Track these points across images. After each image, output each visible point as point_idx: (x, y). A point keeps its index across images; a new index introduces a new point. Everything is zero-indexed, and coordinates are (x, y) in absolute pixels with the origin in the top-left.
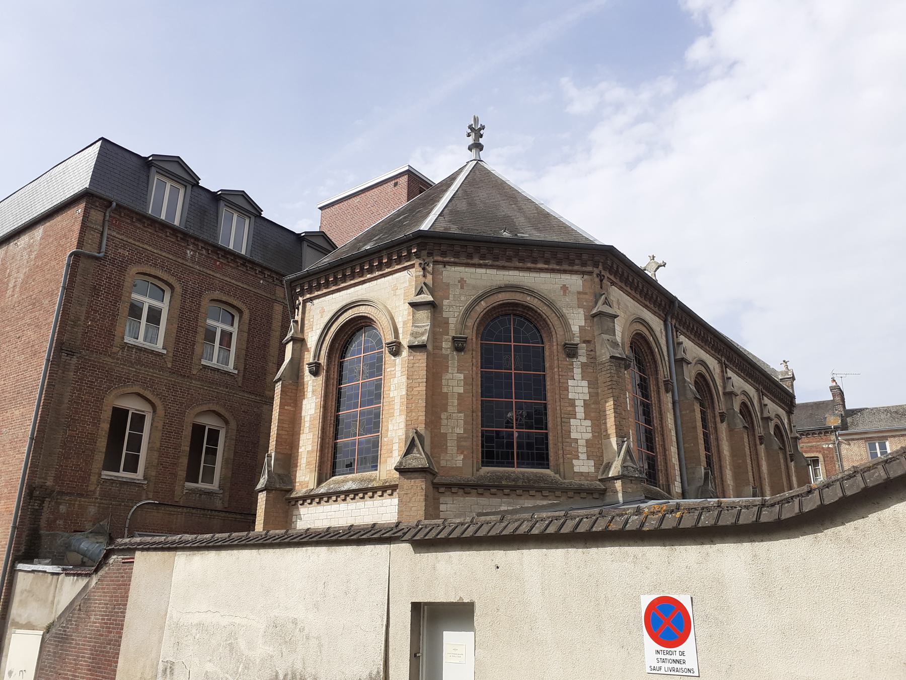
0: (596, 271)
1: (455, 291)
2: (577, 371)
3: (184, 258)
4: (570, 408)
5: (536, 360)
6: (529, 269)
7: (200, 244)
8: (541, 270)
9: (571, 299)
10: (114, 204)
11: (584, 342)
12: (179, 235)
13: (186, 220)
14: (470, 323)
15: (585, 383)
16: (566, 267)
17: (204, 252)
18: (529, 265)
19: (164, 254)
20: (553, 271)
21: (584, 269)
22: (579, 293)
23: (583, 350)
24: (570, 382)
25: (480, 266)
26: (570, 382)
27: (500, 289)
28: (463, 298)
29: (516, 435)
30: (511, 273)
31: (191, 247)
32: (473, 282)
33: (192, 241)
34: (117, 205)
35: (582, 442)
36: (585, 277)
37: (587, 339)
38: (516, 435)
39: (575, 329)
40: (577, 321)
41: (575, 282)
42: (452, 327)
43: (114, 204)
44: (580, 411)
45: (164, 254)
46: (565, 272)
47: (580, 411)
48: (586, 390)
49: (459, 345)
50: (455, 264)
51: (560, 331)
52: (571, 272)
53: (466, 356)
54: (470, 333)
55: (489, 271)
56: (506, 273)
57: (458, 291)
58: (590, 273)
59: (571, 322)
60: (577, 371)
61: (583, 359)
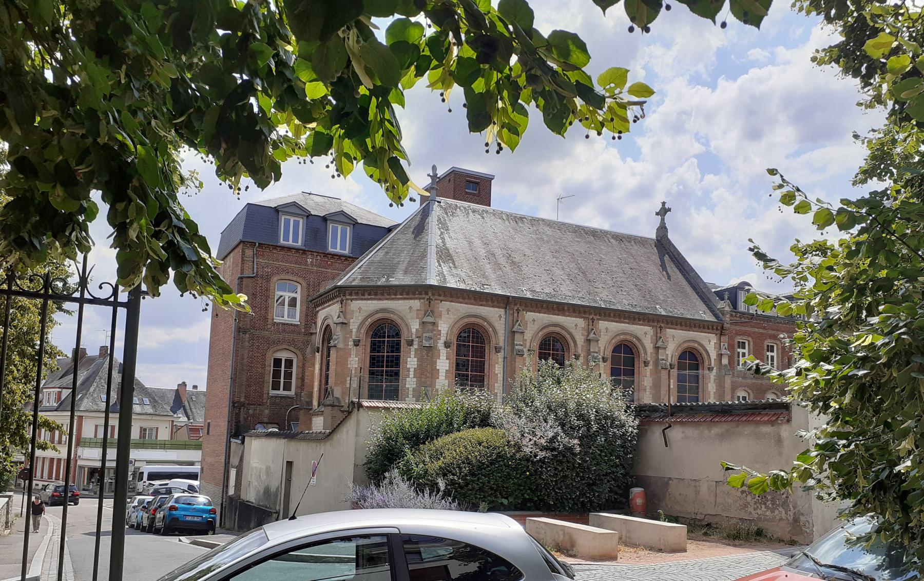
0: (427, 297)
1: (357, 314)
2: (413, 353)
3: (306, 265)
4: (407, 373)
5: (396, 347)
6: (393, 299)
7: (315, 254)
8: (399, 299)
9: (414, 314)
10: (257, 244)
11: (417, 337)
12: (301, 251)
13: (306, 242)
14: (363, 331)
15: (416, 359)
16: (411, 296)
17: (319, 257)
18: (393, 297)
19: (293, 265)
20: (405, 299)
21: (421, 296)
22: (417, 310)
23: (416, 343)
24: (409, 359)
25: (368, 299)
26: (409, 359)
27: (377, 312)
28: (360, 318)
29: (384, 386)
30: (384, 302)
31: (310, 257)
32: (365, 309)
33: (310, 253)
34: (259, 244)
35: (411, 389)
36: (422, 301)
37: (419, 335)
38: (384, 386)
39: (414, 331)
40: (415, 326)
41: (416, 304)
42: (354, 333)
43: (257, 244)
44: (412, 374)
45: (293, 265)
46: (411, 299)
47: (412, 374)
48: (416, 363)
49: (357, 343)
50: (356, 299)
51: (406, 332)
52: (414, 299)
53: (360, 348)
54: (362, 337)
55: (373, 302)
56: (382, 302)
57: (358, 314)
58: (424, 298)
59: (412, 327)
60: (413, 353)
61: (416, 346)
